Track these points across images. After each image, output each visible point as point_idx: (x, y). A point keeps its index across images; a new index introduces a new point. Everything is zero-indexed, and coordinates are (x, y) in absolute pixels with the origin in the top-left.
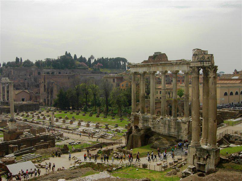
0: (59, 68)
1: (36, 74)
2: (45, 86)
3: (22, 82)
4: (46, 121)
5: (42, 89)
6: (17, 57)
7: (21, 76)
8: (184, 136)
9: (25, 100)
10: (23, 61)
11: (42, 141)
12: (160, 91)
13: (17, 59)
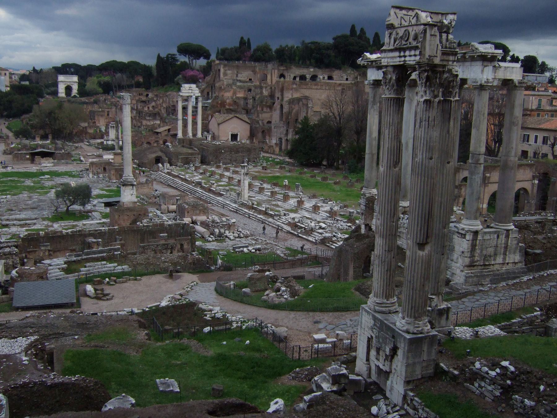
1: (275, 78)
2: (282, 106)
3: (241, 95)
5: (276, 116)
7: (240, 81)
8: (458, 272)
11: (163, 236)
12: (544, 137)
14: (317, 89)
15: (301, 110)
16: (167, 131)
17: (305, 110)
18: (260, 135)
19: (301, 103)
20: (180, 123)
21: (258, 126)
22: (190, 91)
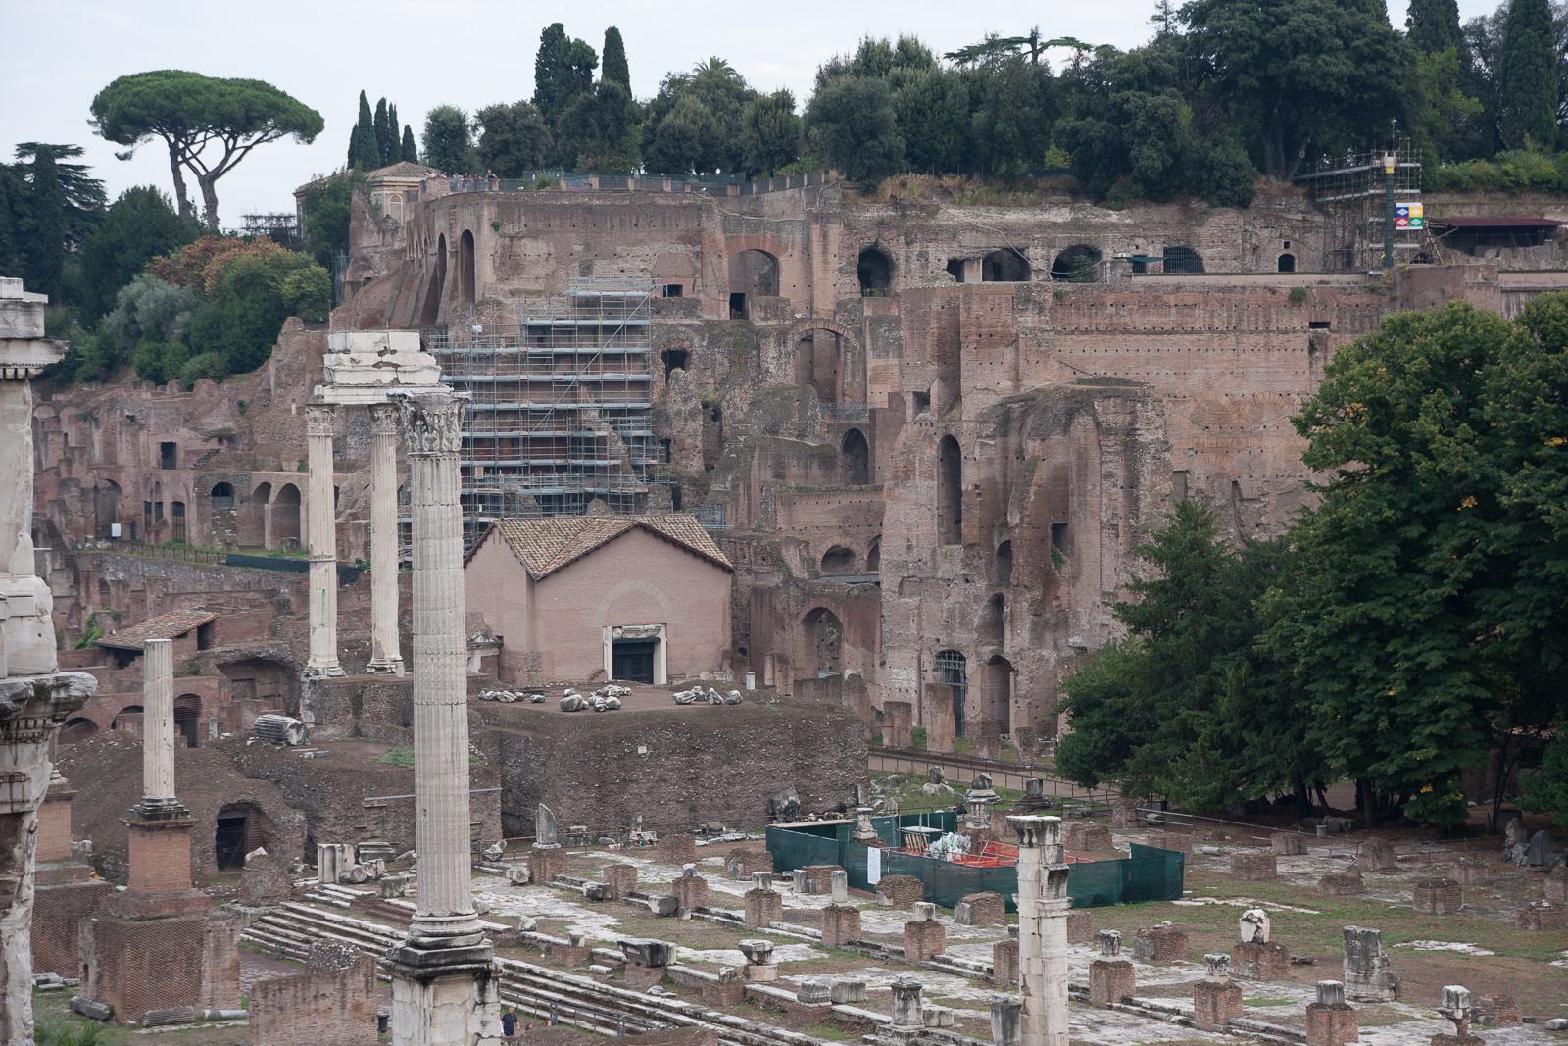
0: (1157, 190)
4: (957, 988)
5: (910, 512)
6: (553, 36)
9: (661, 676)
10: (644, 88)
13: (559, 56)
14: (1154, 332)
15: (1083, 465)
16: (192, 641)
17: (1116, 466)
18: (793, 639)
19: (1084, 421)
20: (323, 581)
21: (776, 580)
22: (387, 376)
